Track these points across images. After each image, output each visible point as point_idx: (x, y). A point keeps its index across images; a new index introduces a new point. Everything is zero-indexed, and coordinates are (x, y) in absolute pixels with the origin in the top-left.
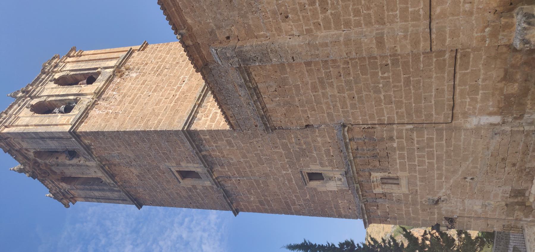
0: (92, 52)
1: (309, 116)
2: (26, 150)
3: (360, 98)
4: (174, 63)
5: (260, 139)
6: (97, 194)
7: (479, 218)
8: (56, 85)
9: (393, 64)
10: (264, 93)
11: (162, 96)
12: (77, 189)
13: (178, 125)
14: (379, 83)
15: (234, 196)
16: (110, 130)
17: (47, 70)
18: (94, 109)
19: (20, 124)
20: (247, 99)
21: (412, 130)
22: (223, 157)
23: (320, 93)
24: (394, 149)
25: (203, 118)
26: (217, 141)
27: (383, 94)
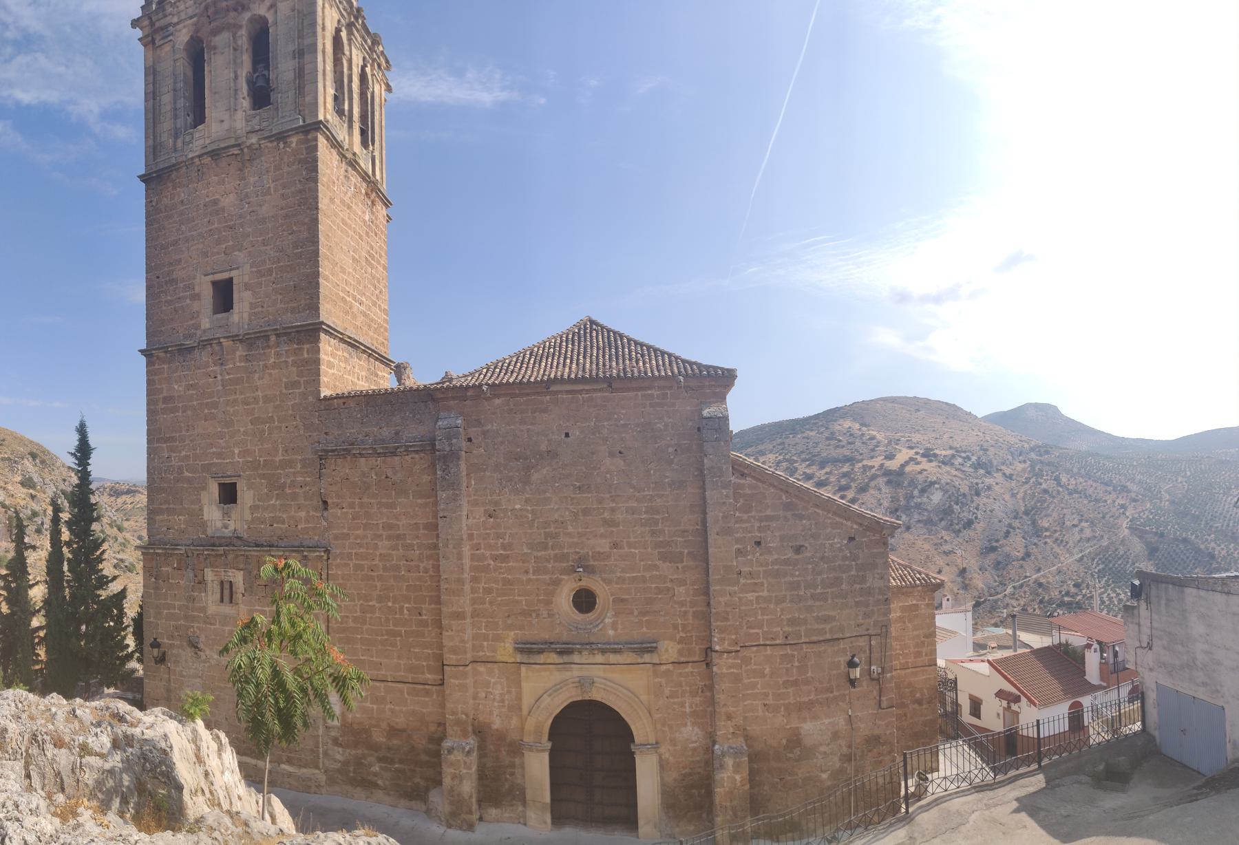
1: (344, 510)
3: (372, 578)
5: (302, 432)
9: (421, 621)
10: (384, 462)
14: (394, 603)
15: (182, 359)
16: (320, 195)
20: (375, 436)
22: (265, 366)
23: (381, 532)
26: (298, 367)
27: (377, 605)
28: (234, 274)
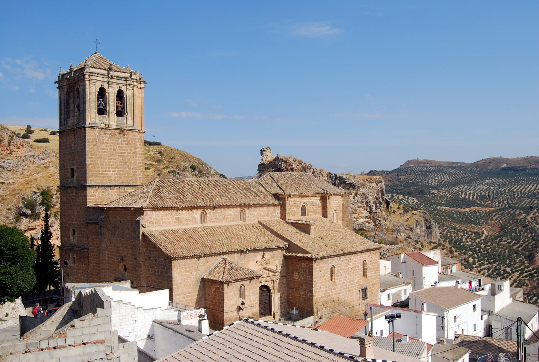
0: (143, 96)
2: (79, 86)
4: (126, 161)
6: (63, 108)
8: (116, 92)
11: (106, 164)
12: (64, 96)
18: (99, 130)
19: (91, 88)
21: (87, 272)
24: (82, 264)
28: (74, 167)
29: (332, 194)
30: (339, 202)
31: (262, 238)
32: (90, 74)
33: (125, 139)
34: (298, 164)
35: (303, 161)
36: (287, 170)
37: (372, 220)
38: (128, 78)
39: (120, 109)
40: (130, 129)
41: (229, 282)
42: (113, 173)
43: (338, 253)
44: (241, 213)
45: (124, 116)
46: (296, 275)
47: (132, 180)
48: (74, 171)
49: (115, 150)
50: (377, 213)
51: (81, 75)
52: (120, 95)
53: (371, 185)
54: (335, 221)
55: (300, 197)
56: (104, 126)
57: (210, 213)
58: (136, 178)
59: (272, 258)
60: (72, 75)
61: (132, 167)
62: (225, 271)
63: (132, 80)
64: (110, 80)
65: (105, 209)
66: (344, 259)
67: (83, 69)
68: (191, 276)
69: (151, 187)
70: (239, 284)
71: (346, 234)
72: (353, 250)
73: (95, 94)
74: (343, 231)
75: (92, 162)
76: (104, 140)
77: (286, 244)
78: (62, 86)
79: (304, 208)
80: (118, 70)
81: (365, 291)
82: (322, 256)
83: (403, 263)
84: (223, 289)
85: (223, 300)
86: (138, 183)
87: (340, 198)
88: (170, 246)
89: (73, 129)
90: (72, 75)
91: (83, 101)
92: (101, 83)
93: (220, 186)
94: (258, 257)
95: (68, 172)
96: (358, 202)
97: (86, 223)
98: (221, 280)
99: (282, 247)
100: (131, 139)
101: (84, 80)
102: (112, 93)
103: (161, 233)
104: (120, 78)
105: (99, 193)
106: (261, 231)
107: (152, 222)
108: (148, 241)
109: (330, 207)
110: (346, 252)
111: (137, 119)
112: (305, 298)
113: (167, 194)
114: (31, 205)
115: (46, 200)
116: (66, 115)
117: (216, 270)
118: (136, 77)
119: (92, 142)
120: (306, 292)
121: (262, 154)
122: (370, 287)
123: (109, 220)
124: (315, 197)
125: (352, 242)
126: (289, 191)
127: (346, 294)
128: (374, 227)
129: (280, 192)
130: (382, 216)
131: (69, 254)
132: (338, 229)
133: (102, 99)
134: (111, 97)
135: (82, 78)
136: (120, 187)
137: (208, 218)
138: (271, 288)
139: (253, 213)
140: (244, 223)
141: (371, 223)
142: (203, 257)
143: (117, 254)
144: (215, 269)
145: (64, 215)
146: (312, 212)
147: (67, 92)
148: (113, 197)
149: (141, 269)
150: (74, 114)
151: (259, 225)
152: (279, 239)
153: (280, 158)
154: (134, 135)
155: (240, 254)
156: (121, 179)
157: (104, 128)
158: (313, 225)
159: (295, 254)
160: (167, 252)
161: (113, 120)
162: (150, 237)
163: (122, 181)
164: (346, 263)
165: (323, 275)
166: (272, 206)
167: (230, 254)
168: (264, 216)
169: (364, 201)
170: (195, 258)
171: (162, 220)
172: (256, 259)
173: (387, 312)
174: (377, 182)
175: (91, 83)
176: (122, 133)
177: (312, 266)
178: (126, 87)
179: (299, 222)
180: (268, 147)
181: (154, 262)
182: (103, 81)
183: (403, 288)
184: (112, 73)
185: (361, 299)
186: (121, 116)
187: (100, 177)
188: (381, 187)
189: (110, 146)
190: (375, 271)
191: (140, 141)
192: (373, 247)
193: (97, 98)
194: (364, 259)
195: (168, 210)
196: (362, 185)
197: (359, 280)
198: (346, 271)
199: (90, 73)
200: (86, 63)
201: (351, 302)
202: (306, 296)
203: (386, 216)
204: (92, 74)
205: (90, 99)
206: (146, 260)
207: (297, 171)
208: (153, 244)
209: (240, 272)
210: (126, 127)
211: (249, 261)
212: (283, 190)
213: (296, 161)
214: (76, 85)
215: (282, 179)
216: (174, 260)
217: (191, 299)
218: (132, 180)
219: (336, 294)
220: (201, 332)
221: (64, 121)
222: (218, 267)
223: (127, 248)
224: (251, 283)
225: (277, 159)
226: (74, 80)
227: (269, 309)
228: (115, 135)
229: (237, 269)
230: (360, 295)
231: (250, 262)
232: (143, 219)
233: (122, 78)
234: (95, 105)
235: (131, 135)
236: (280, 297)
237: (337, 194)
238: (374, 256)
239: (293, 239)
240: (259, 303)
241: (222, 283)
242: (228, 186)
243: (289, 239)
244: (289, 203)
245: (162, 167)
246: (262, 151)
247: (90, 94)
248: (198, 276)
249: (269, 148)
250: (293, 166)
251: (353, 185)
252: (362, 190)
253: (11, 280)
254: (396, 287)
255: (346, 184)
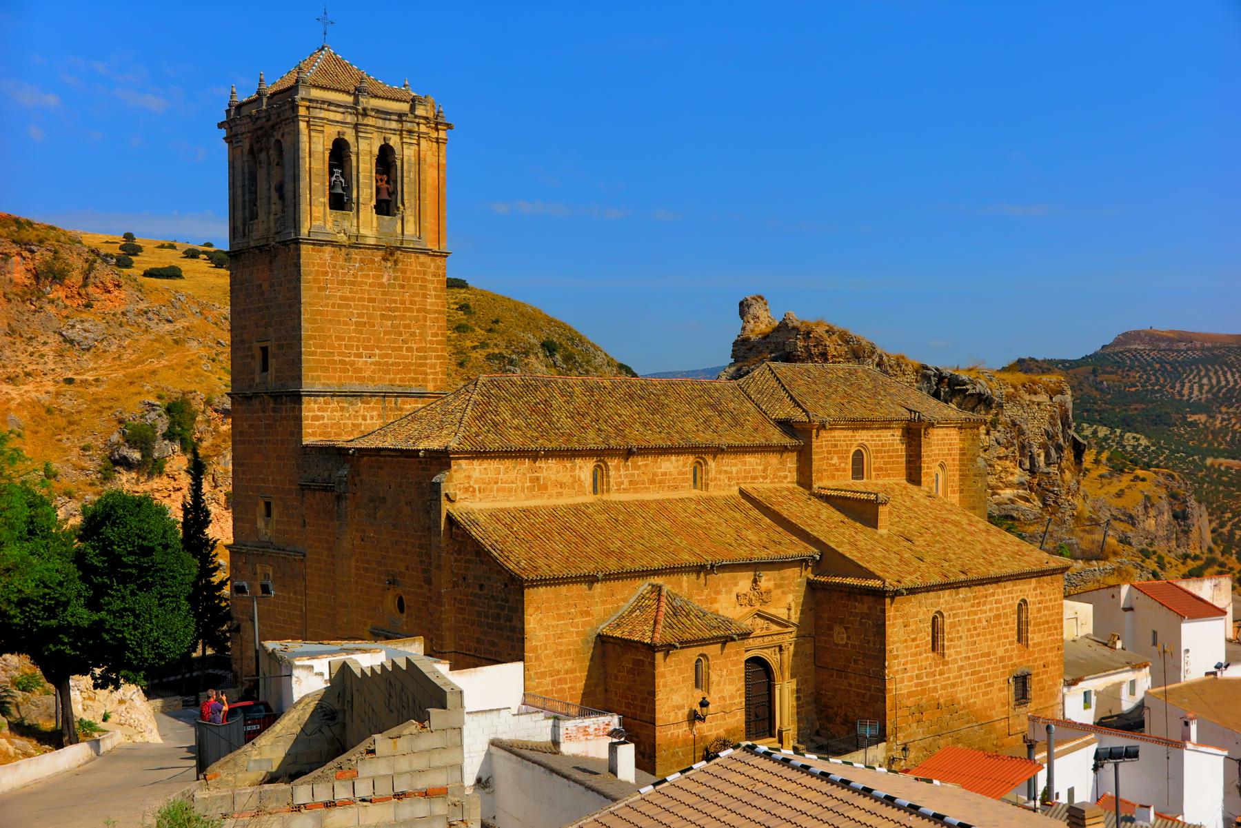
2: (283, 136)
4: (401, 329)
6: (239, 191)
7: (241, 653)
8: (376, 151)
12: (243, 162)
13: (305, 388)
17: (404, 118)
18: (333, 249)
19: (314, 140)
21: (302, 611)
25: (316, 406)
28: (268, 344)
29: (936, 422)
30: (951, 444)
31: (751, 535)
32: (311, 105)
33: (399, 274)
34: (840, 342)
35: (852, 333)
36: (810, 357)
37: (1036, 493)
38: (406, 115)
39: (385, 196)
40: (412, 246)
41: (668, 648)
42: (367, 362)
43: (952, 579)
44: (695, 469)
45: (395, 215)
46: (839, 633)
47: (415, 380)
48: (270, 355)
49: (371, 300)
50: (1049, 473)
51: (287, 107)
52: (386, 160)
53: (1035, 399)
54: (940, 493)
55: (849, 429)
56: (345, 238)
57: (617, 468)
58: (426, 374)
59: (777, 586)
60: (264, 107)
61: (415, 346)
62: (659, 617)
63: (417, 120)
64: (361, 121)
65: (351, 452)
66: (969, 594)
67: (293, 89)
68: (572, 629)
69: (467, 398)
70: (693, 653)
71: (973, 528)
72: (994, 572)
73: (322, 156)
74: (965, 521)
75: (315, 331)
76: (343, 274)
77: (814, 552)
78: (236, 135)
79: (858, 458)
80: (380, 93)
81: (1022, 683)
82: (910, 585)
83: (1125, 610)
84: (653, 665)
85: (653, 694)
86: (430, 388)
87: (953, 436)
88: (517, 549)
89: (267, 245)
90: (264, 107)
91: (291, 173)
92: (338, 128)
93: (642, 398)
94: (741, 583)
95: (253, 357)
96: (999, 444)
97: (299, 487)
98: (648, 641)
99: (804, 560)
100: (414, 273)
101: (295, 119)
102: (365, 155)
103: (495, 516)
104: (383, 114)
105: (332, 412)
106: (747, 516)
107: (471, 489)
108: (463, 536)
109: (928, 456)
110: (973, 576)
111: (429, 223)
112: (863, 696)
113: (507, 416)
114: (141, 439)
115: (179, 425)
116: (247, 212)
117: (633, 615)
118: (427, 111)
119: (316, 280)
120: (867, 678)
121: (742, 314)
122: (1035, 671)
123: (361, 481)
124: (890, 428)
125: (990, 551)
126: (821, 412)
127: (973, 689)
128: (1040, 511)
129: (799, 416)
130: (1063, 481)
131: (254, 568)
132: (950, 516)
133: (339, 168)
134: (364, 163)
135: (289, 114)
136: (384, 397)
137: (611, 480)
138: (775, 667)
139: (726, 468)
140: (704, 494)
141: (1034, 500)
142: (603, 580)
143: (380, 568)
144: (632, 612)
145: (242, 465)
146: (881, 469)
147: (251, 151)
148: (369, 421)
149: (443, 609)
150: (270, 209)
151: (743, 501)
152: (794, 538)
153: (790, 325)
154: (422, 264)
155: (695, 575)
156: (387, 376)
157: (347, 243)
158: (885, 504)
159: (837, 580)
160: (511, 566)
161: (367, 224)
162: (468, 527)
163: (390, 381)
164: (972, 607)
165: (913, 636)
166: (776, 451)
167: (670, 574)
168: (756, 478)
169: (1015, 441)
170: (581, 582)
171: (496, 483)
172: (736, 590)
173: (1084, 740)
174: (1052, 390)
175: (312, 127)
176: (390, 258)
177: (884, 611)
178: (402, 138)
179: (849, 494)
180: (759, 297)
181: (477, 591)
182: (342, 123)
183: (1126, 676)
184: (365, 102)
185: (1013, 703)
186: (388, 215)
187: (335, 370)
188: (1061, 406)
189: (361, 290)
190: (1050, 629)
191: (435, 279)
192: (1045, 567)
193: (327, 166)
194: (1020, 598)
195: (513, 458)
196: (1010, 398)
197: (1006, 651)
198: (972, 627)
199: (310, 101)
200: (301, 75)
201: (985, 709)
202: (865, 689)
203: (1073, 484)
204: (315, 105)
205: (310, 168)
206: (455, 585)
207: (837, 360)
208: (476, 543)
209: (697, 621)
210: (402, 243)
211: (718, 593)
212: (804, 411)
213: (834, 333)
214: (275, 133)
215: (803, 382)
216: (528, 587)
217: (569, 688)
218: (415, 380)
219: (944, 687)
220: (616, 775)
221: (244, 225)
222: (638, 607)
223: (405, 552)
224: (726, 651)
225: (783, 328)
226: (268, 120)
227: (767, 721)
228: (373, 262)
229: (688, 615)
230: (1010, 693)
231: (719, 597)
232: (450, 480)
233: (390, 114)
234: (324, 184)
235: (412, 263)
236: (798, 691)
237: (946, 423)
238: (1047, 589)
239: (832, 539)
240: (744, 704)
241: (651, 649)
242: (662, 398)
243: (822, 538)
244: (821, 443)
245: (468, 344)
246: (744, 307)
247: (310, 157)
248: (588, 629)
249: (762, 299)
250: (825, 345)
251: (987, 397)
252: (1010, 411)
253: (135, 628)
254: (1107, 673)
255: (966, 396)
